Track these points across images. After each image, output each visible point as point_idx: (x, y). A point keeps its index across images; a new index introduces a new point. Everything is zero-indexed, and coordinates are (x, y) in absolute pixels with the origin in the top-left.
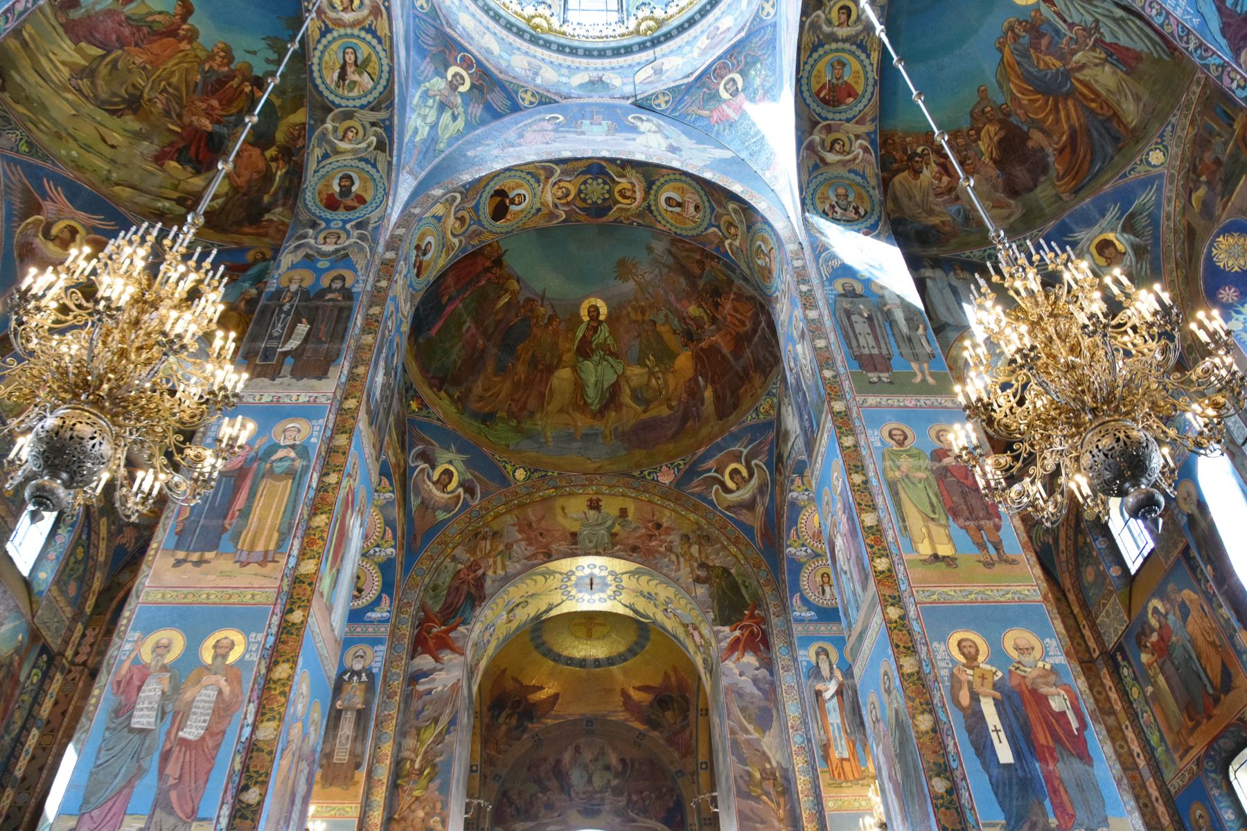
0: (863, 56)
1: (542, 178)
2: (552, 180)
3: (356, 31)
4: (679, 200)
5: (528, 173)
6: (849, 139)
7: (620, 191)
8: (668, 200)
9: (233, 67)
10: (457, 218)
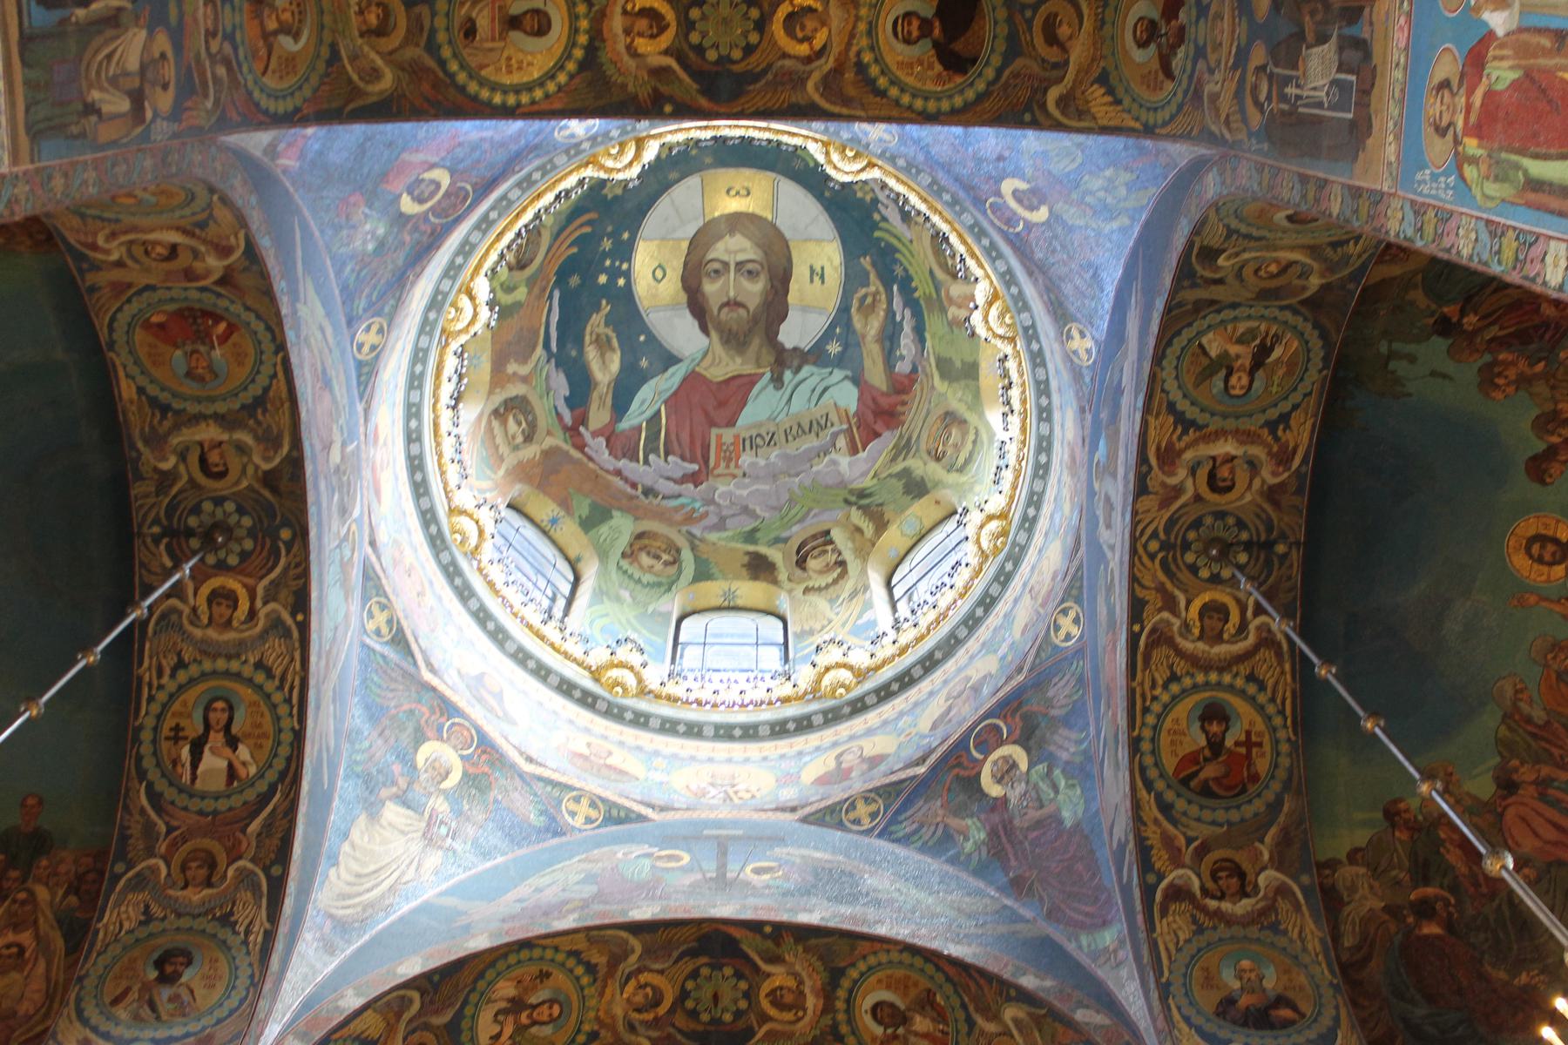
0: (152, 390)
1: (849, 75)
2: (828, 64)
3: (1215, 424)
4: (515, 35)
5: (882, 94)
6: (136, 261)
7: (663, 29)
8: (542, 29)
9: (1487, 358)
10: (1063, 48)
